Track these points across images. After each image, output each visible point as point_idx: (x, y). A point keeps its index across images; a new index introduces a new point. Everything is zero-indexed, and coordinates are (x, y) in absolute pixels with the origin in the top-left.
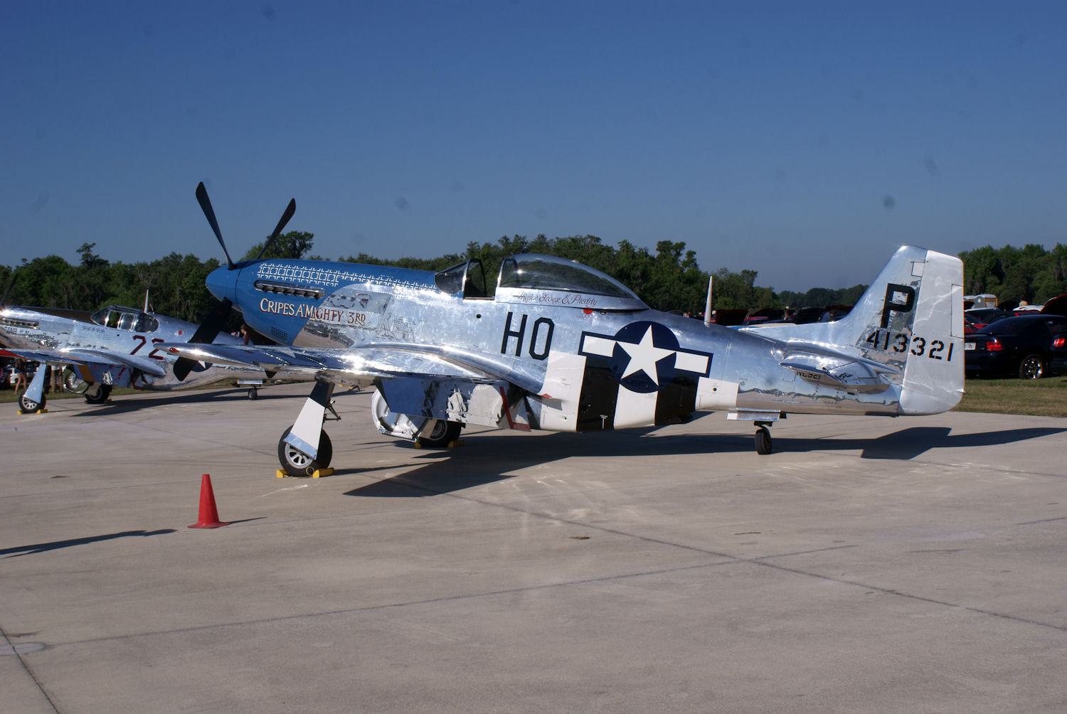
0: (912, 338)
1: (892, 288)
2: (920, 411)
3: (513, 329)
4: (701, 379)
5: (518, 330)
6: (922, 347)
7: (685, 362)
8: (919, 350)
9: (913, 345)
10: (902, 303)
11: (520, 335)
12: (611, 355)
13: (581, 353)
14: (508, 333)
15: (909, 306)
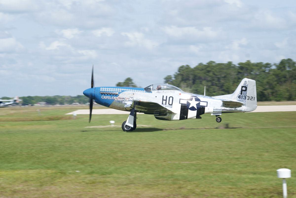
0: (247, 97)
1: (242, 87)
2: (250, 111)
3: (164, 99)
4: (206, 107)
5: (165, 99)
6: (249, 98)
7: (202, 104)
8: (248, 99)
9: (247, 98)
10: (245, 89)
11: (166, 100)
12: (186, 103)
13: (180, 103)
14: (163, 100)
15: (246, 90)
